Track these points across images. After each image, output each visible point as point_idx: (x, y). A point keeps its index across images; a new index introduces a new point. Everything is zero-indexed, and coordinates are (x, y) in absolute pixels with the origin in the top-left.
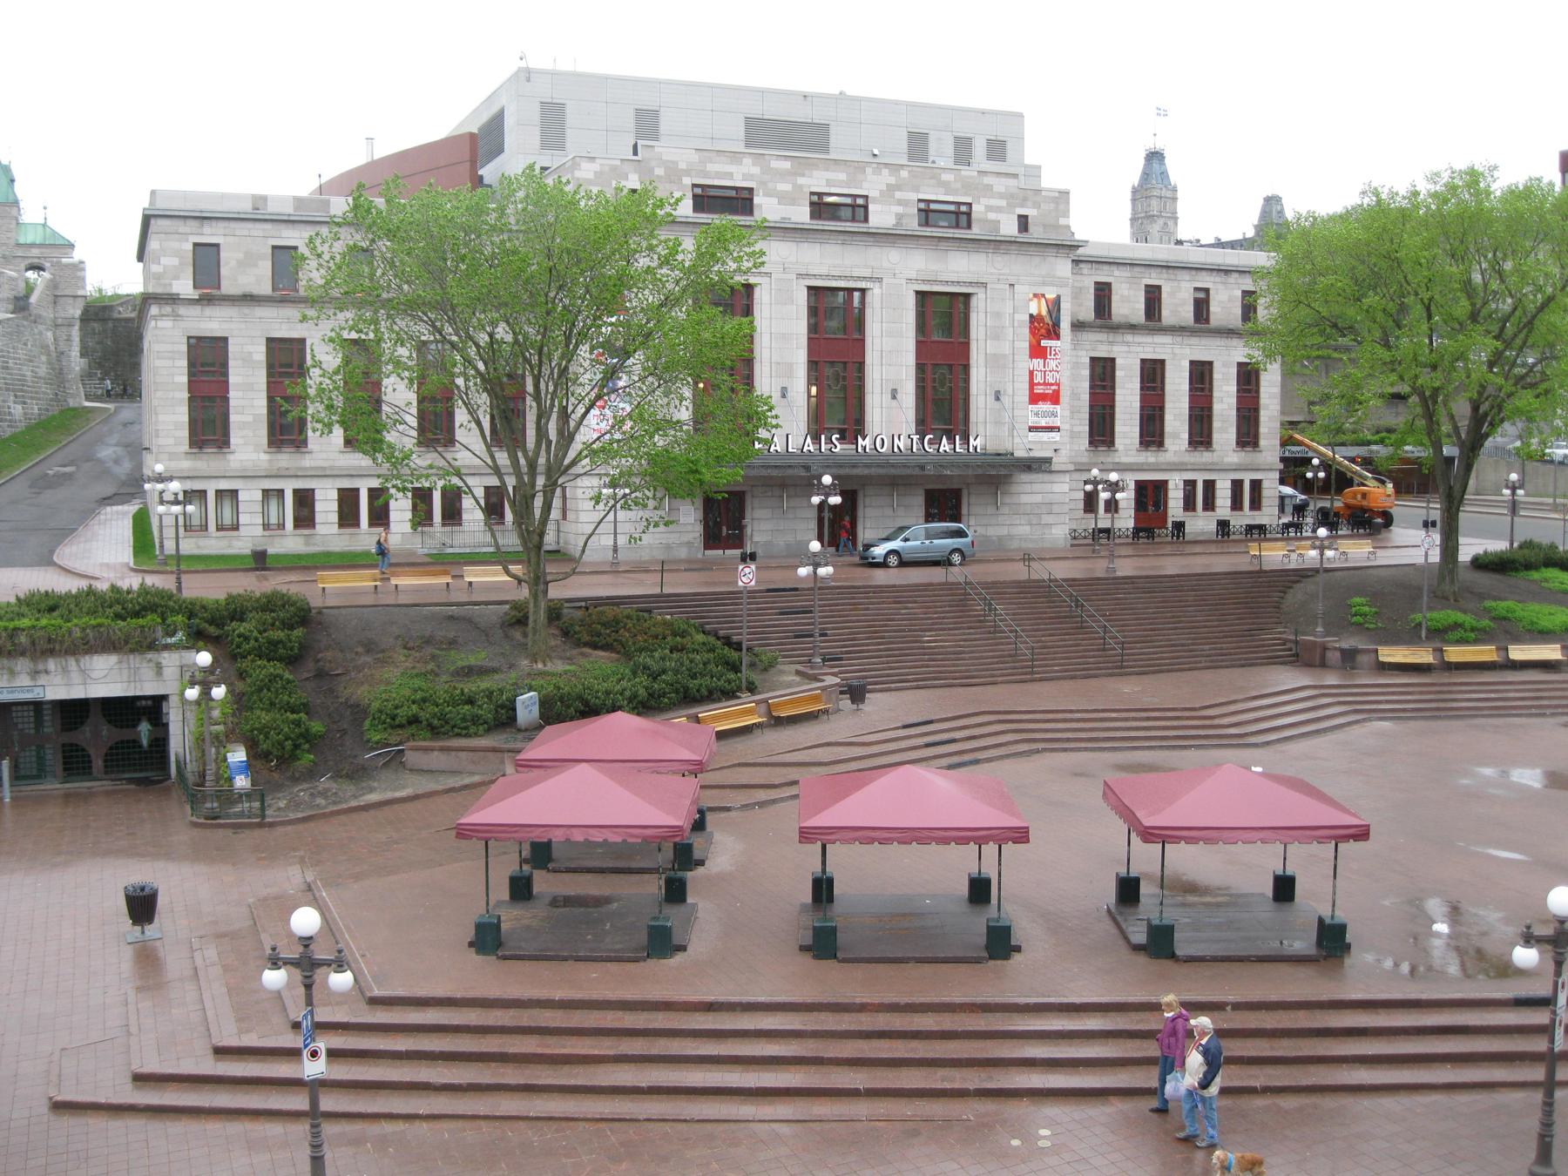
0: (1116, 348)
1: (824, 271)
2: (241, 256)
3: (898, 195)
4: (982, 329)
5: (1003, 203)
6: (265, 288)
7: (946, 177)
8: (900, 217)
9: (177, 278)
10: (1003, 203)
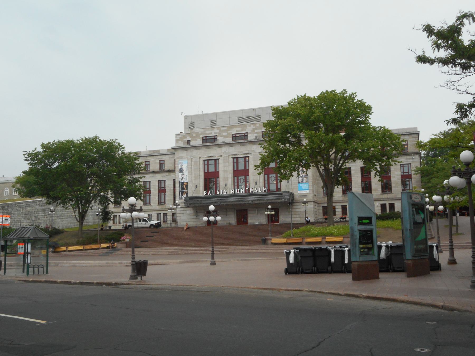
1: (235, 153)
3: (256, 131)
8: (256, 137)
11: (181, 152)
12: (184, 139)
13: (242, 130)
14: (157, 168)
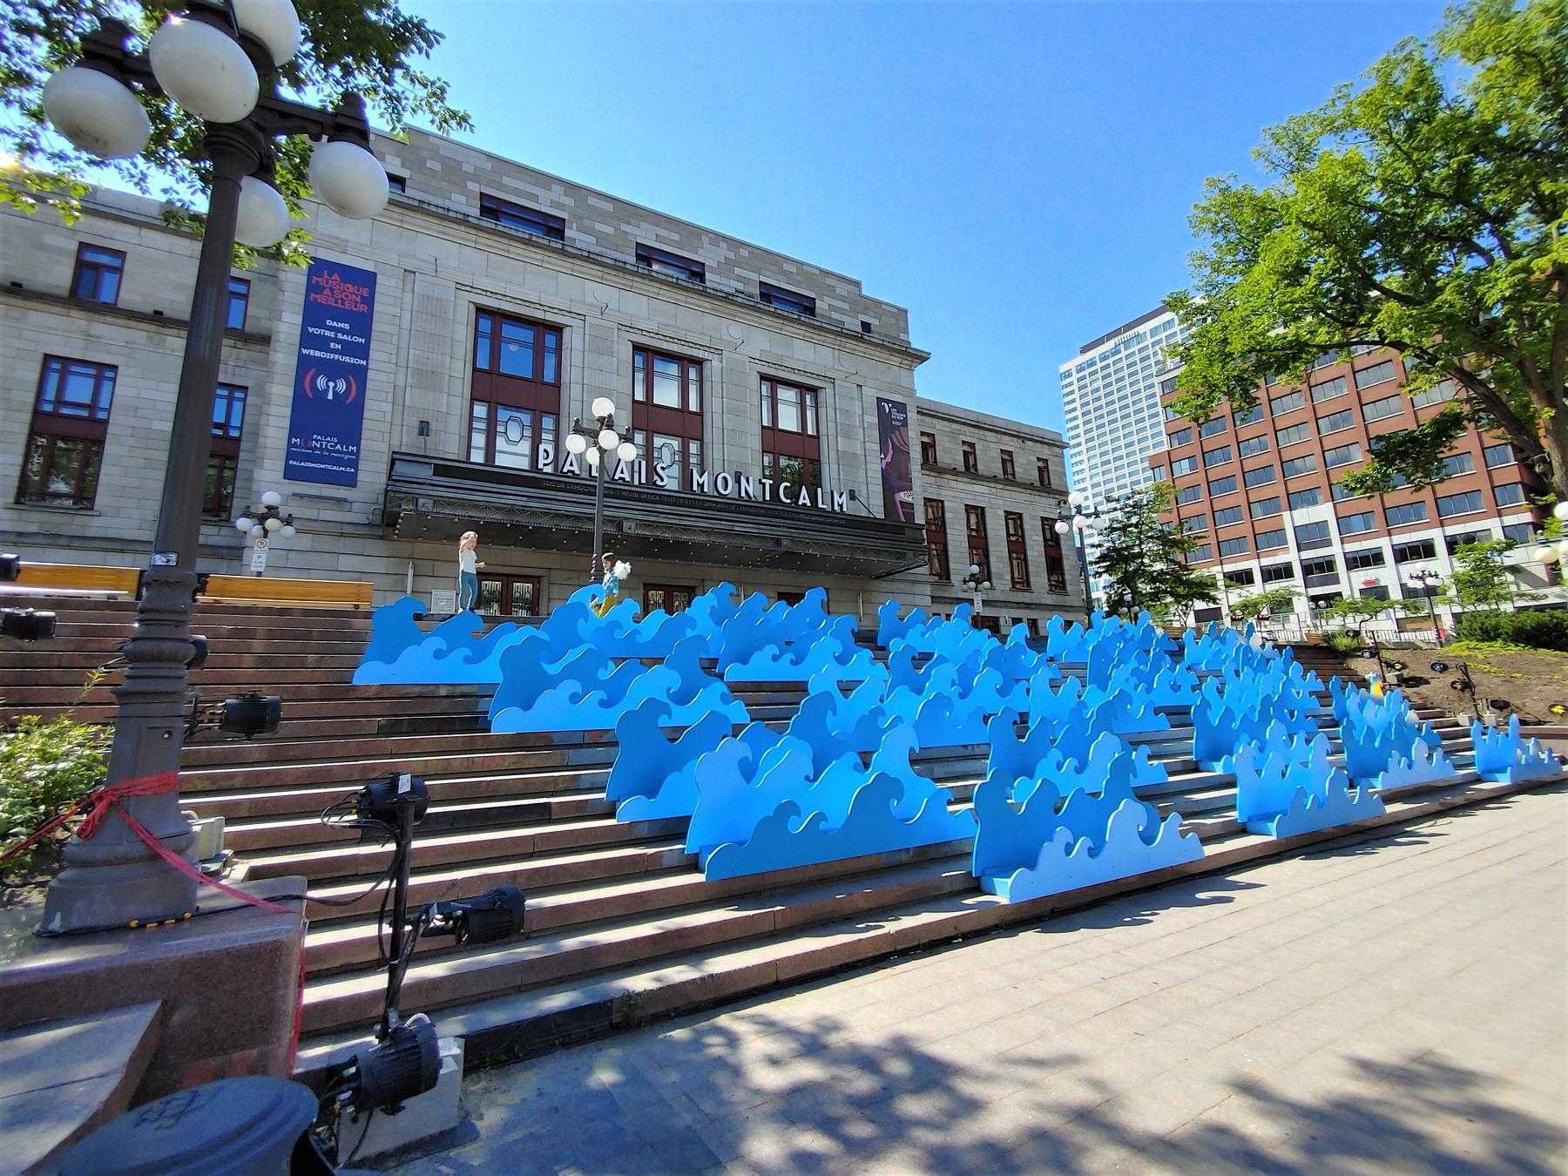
0: (943, 492)
1: (654, 328)
4: (831, 425)
5: (846, 306)
7: (787, 267)
10: (846, 306)
13: (680, 246)
14: (60, 275)
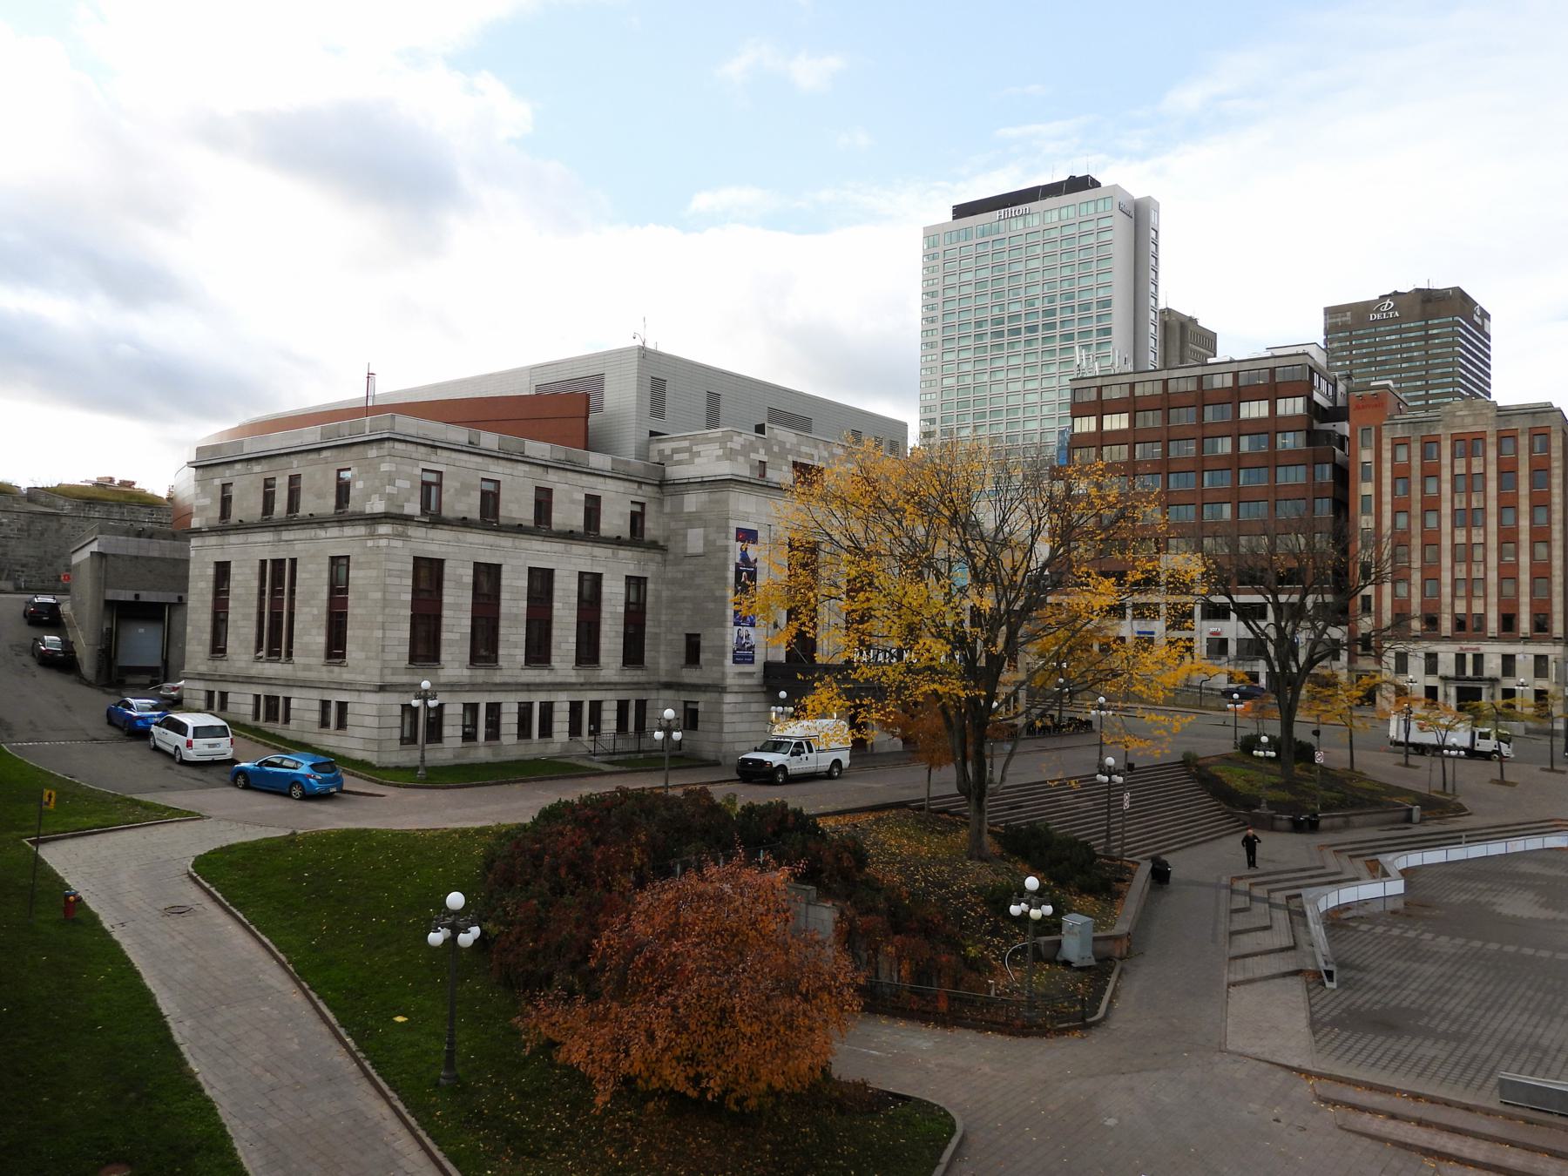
2: (458, 485)
6: (475, 515)
9: (408, 500)
11: (743, 497)
12: (753, 456)
